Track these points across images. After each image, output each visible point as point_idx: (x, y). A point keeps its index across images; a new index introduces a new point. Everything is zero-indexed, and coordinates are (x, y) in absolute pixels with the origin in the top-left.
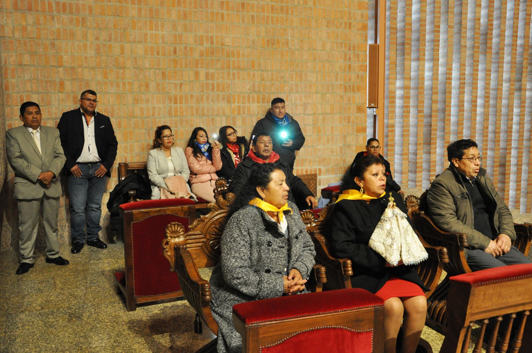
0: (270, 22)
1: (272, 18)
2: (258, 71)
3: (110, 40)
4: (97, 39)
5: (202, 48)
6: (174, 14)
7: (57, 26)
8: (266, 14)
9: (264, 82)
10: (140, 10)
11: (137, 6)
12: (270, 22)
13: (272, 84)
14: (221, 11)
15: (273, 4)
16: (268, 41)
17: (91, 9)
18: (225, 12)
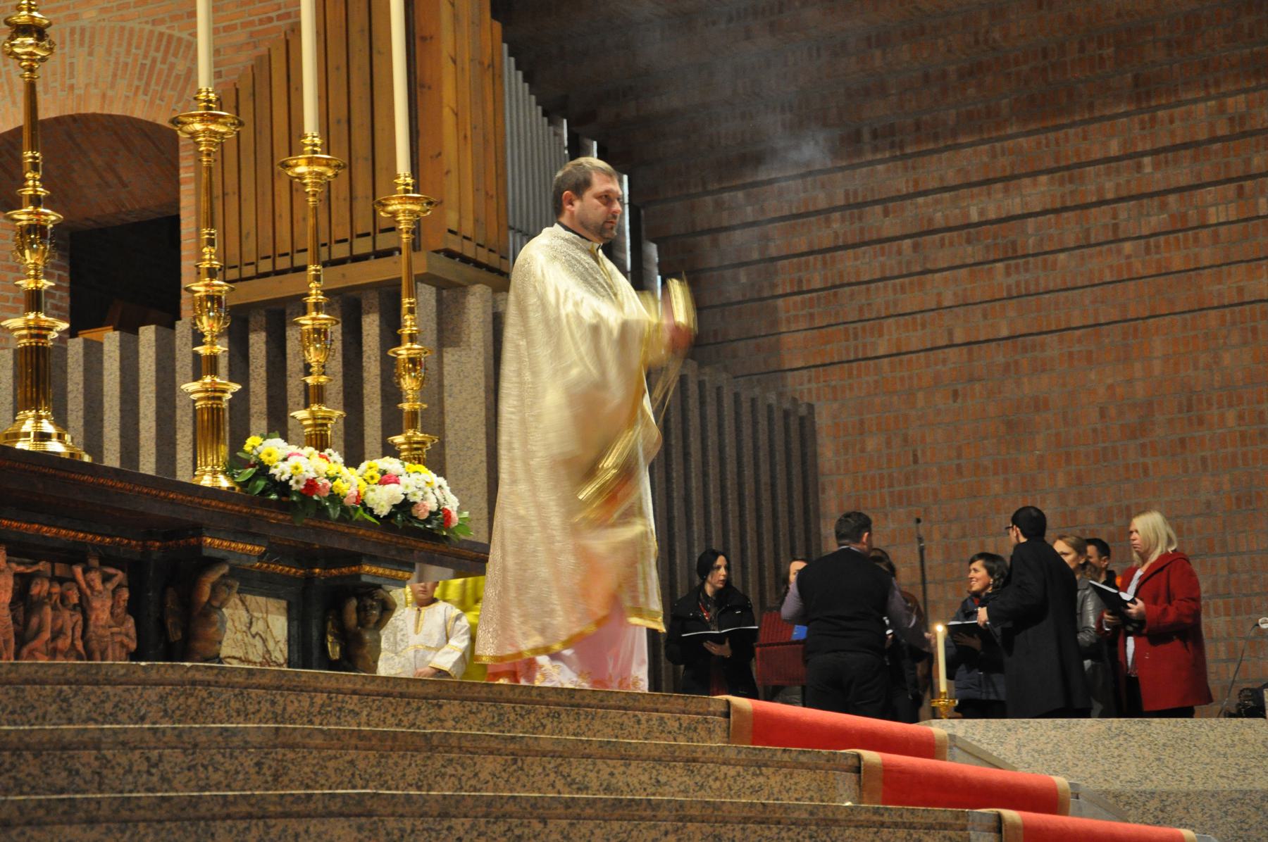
0: (1240, 462)
1: (1245, 454)
2: (1222, 555)
3: (964, 536)
4: (946, 536)
5: (1112, 528)
6: (1061, 481)
7: (892, 526)
8: (1230, 449)
9: (1235, 575)
10: (1006, 481)
11: (1001, 477)
12: (1240, 462)
13: (1254, 578)
14: (1141, 460)
15: (1242, 428)
16: (1238, 499)
17: (935, 494)
18: (1149, 461)
